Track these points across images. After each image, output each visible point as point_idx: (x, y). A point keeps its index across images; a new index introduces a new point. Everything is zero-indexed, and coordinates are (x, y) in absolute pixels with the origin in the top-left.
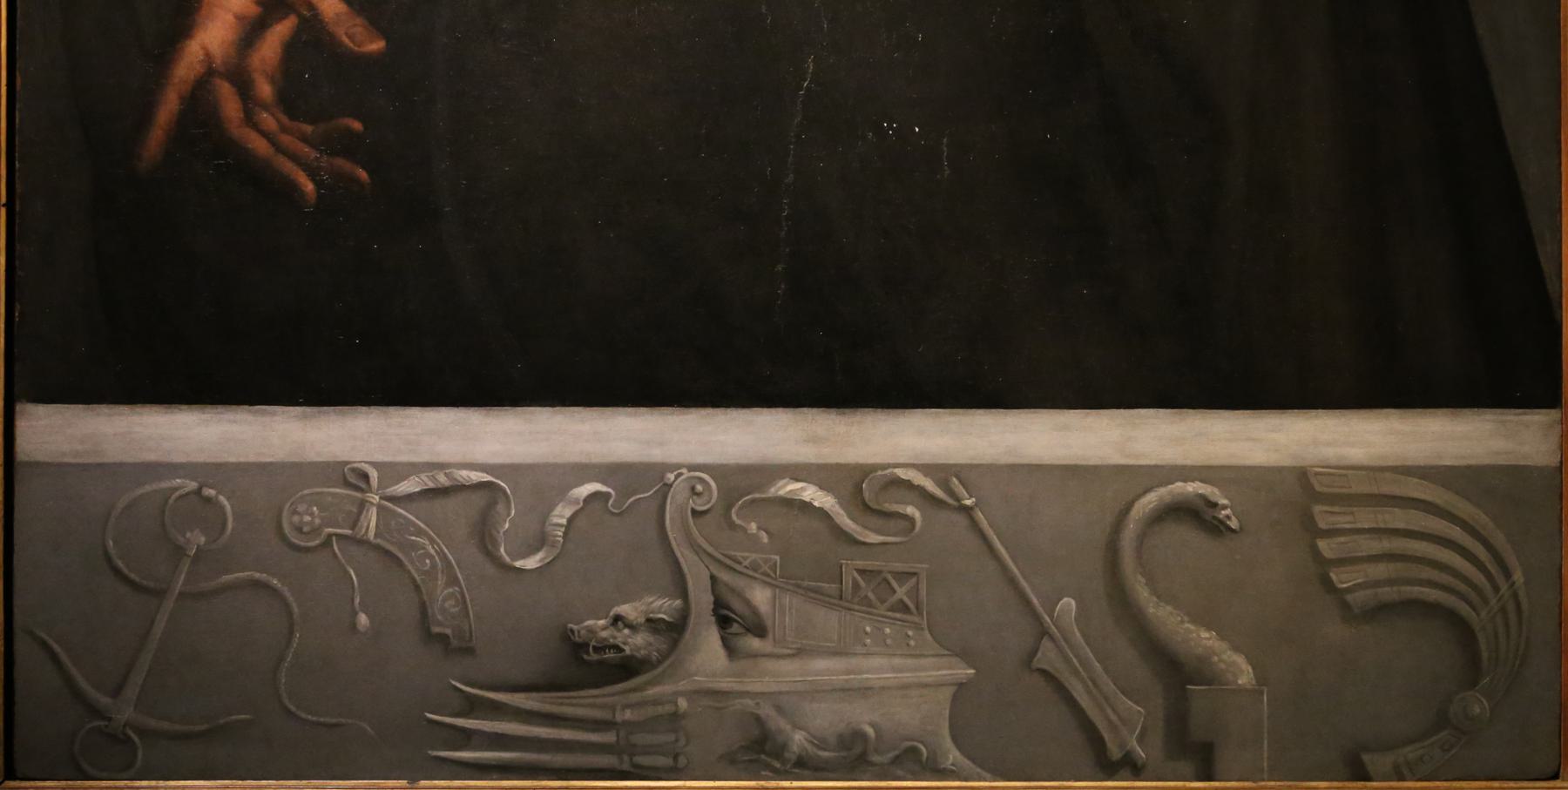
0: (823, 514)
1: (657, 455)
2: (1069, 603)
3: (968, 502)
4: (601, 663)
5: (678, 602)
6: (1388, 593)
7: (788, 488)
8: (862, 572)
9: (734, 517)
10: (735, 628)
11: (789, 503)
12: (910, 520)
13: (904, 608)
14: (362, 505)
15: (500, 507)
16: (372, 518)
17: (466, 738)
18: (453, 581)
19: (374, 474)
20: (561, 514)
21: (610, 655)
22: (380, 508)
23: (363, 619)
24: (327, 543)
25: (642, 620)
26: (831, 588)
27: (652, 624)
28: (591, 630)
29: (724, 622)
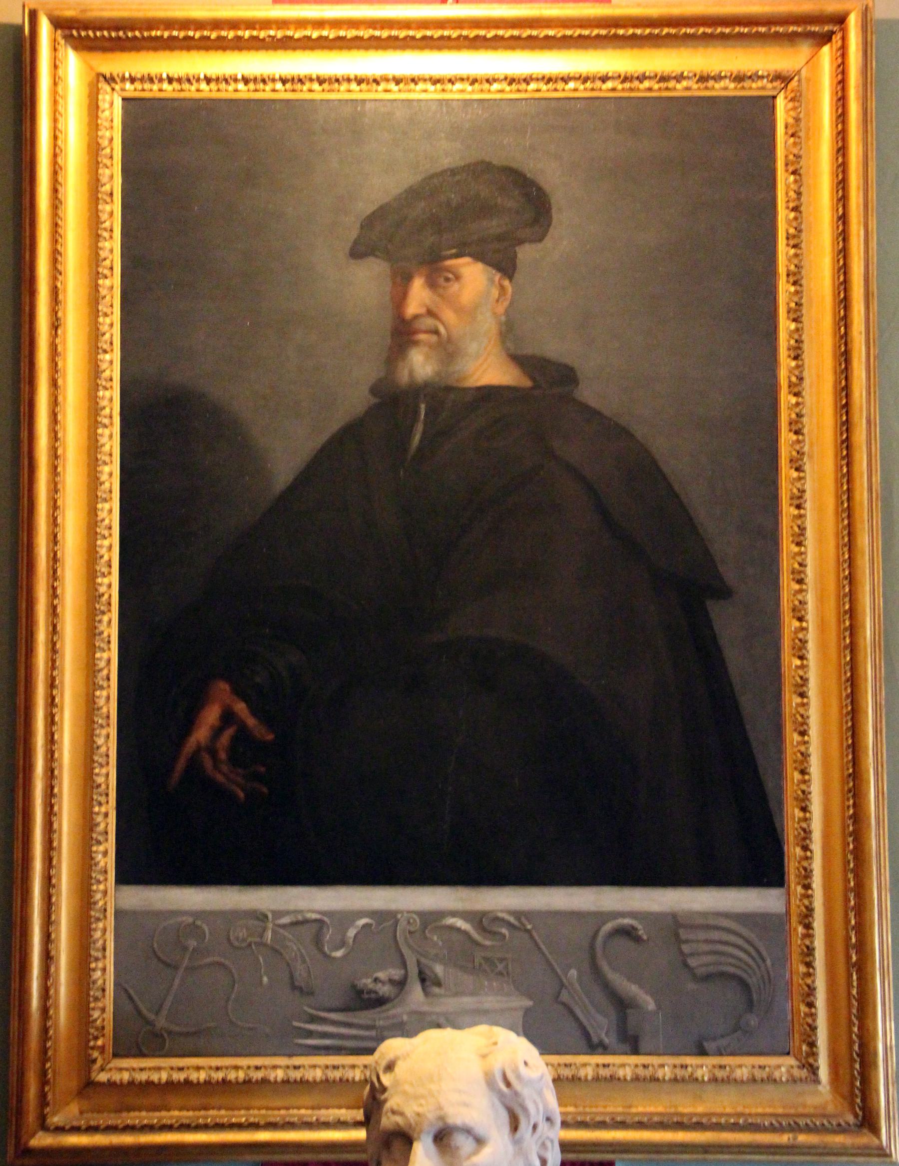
0: (465, 933)
1: (393, 907)
2: (573, 973)
3: (529, 927)
4: (369, 999)
5: (403, 972)
6: (711, 969)
7: (450, 921)
8: (484, 958)
9: (428, 935)
10: (428, 983)
11: (452, 928)
12: (505, 936)
13: (501, 974)
14: (265, 929)
15: (325, 930)
16: (269, 935)
17: (310, 1034)
18: (304, 962)
19: (270, 916)
20: (351, 933)
21: (373, 996)
22: (273, 931)
23: (265, 979)
24: (250, 945)
25: (387, 979)
26: (470, 965)
27: (391, 981)
28: (365, 984)
29: (423, 980)
